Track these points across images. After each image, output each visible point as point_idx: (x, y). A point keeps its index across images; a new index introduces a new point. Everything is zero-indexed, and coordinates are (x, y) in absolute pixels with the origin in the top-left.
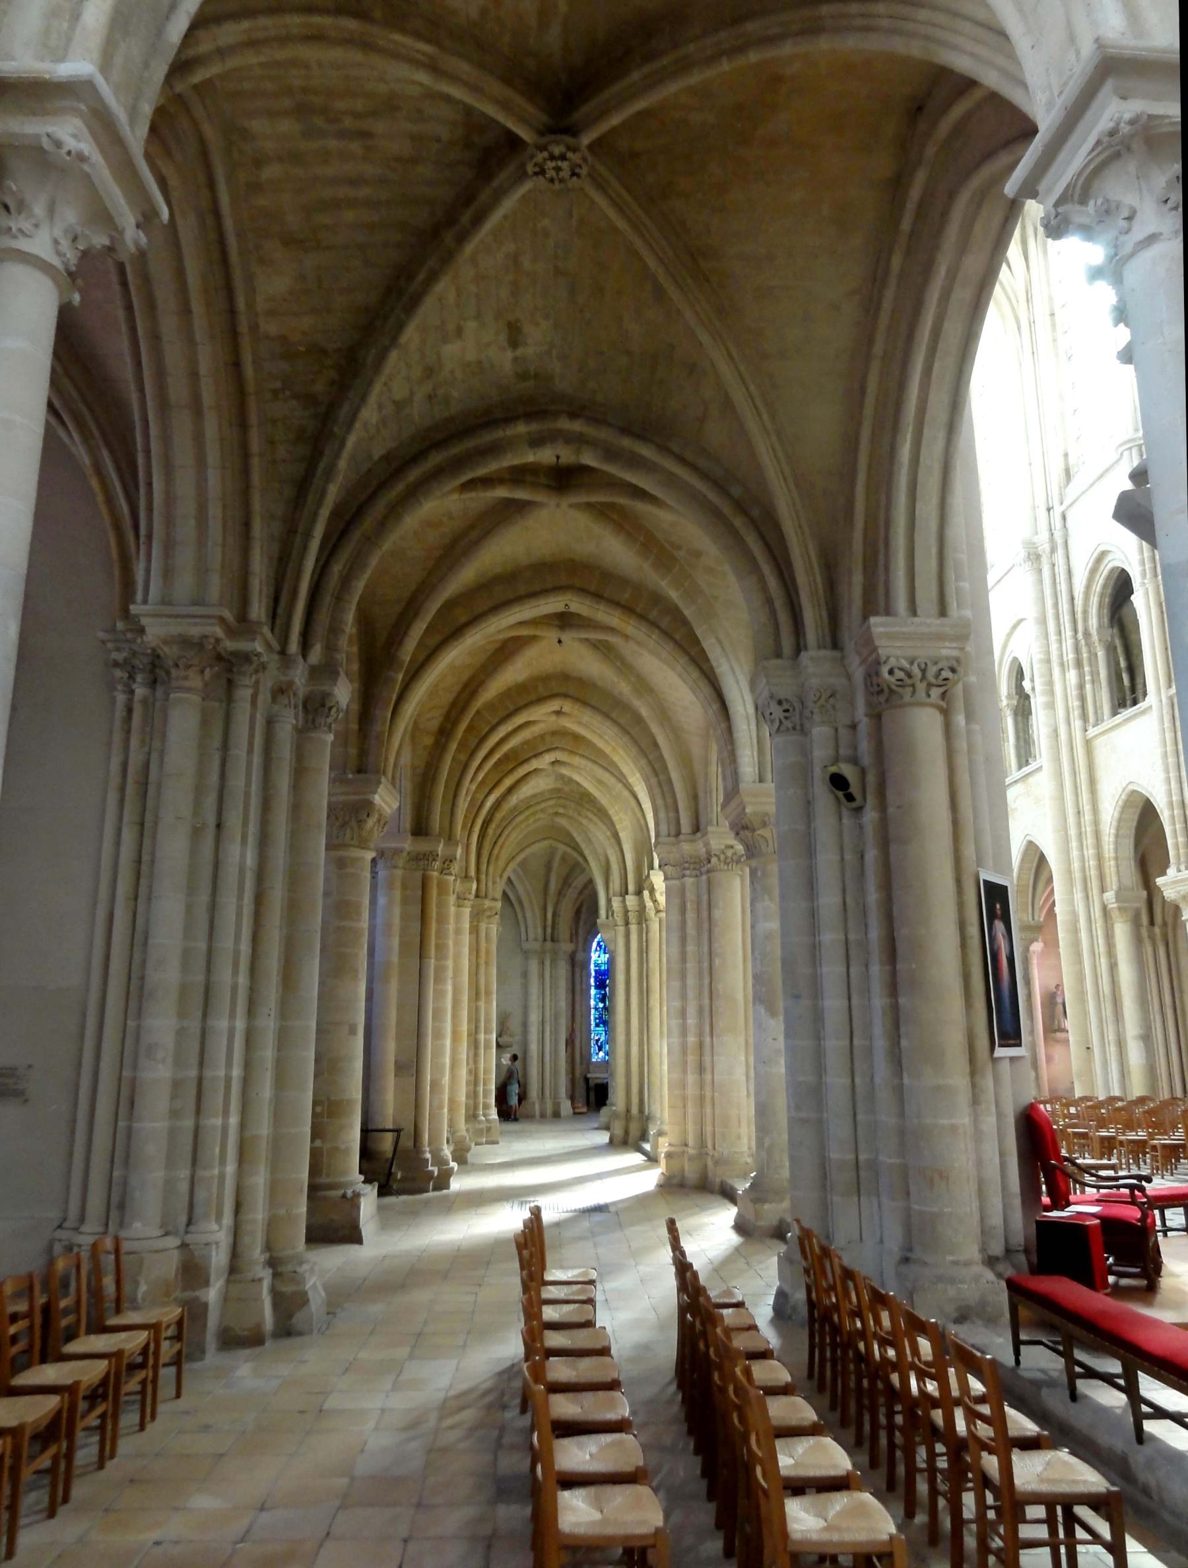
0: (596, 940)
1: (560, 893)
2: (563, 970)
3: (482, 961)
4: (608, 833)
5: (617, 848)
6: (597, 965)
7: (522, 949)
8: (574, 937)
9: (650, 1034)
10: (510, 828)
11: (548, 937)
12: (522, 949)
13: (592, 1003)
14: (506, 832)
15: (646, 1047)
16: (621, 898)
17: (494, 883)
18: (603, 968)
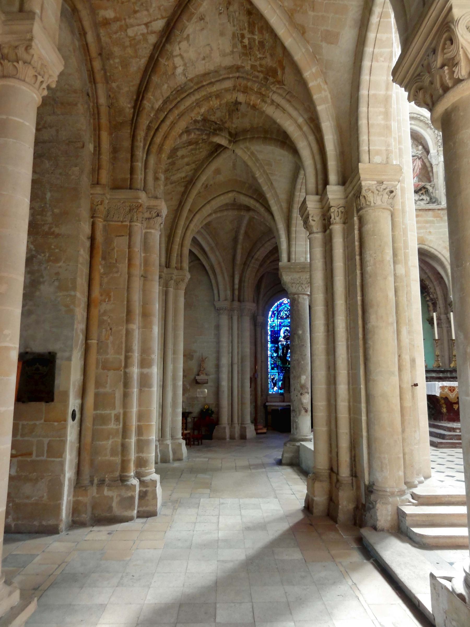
0: (271, 310)
1: (245, 264)
2: (247, 324)
3: (137, 271)
4: (300, 120)
5: (311, 138)
6: (272, 327)
7: (215, 307)
8: (256, 300)
9: (372, 367)
10: (176, 112)
11: (236, 298)
12: (215, 307)
13: (269, 353)
14: (171, 118)
15: (363, 386)
16: (317, 197)
17: (156, 179)
18: (276, 329)
